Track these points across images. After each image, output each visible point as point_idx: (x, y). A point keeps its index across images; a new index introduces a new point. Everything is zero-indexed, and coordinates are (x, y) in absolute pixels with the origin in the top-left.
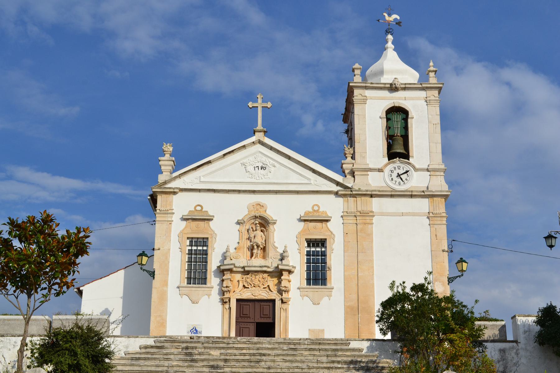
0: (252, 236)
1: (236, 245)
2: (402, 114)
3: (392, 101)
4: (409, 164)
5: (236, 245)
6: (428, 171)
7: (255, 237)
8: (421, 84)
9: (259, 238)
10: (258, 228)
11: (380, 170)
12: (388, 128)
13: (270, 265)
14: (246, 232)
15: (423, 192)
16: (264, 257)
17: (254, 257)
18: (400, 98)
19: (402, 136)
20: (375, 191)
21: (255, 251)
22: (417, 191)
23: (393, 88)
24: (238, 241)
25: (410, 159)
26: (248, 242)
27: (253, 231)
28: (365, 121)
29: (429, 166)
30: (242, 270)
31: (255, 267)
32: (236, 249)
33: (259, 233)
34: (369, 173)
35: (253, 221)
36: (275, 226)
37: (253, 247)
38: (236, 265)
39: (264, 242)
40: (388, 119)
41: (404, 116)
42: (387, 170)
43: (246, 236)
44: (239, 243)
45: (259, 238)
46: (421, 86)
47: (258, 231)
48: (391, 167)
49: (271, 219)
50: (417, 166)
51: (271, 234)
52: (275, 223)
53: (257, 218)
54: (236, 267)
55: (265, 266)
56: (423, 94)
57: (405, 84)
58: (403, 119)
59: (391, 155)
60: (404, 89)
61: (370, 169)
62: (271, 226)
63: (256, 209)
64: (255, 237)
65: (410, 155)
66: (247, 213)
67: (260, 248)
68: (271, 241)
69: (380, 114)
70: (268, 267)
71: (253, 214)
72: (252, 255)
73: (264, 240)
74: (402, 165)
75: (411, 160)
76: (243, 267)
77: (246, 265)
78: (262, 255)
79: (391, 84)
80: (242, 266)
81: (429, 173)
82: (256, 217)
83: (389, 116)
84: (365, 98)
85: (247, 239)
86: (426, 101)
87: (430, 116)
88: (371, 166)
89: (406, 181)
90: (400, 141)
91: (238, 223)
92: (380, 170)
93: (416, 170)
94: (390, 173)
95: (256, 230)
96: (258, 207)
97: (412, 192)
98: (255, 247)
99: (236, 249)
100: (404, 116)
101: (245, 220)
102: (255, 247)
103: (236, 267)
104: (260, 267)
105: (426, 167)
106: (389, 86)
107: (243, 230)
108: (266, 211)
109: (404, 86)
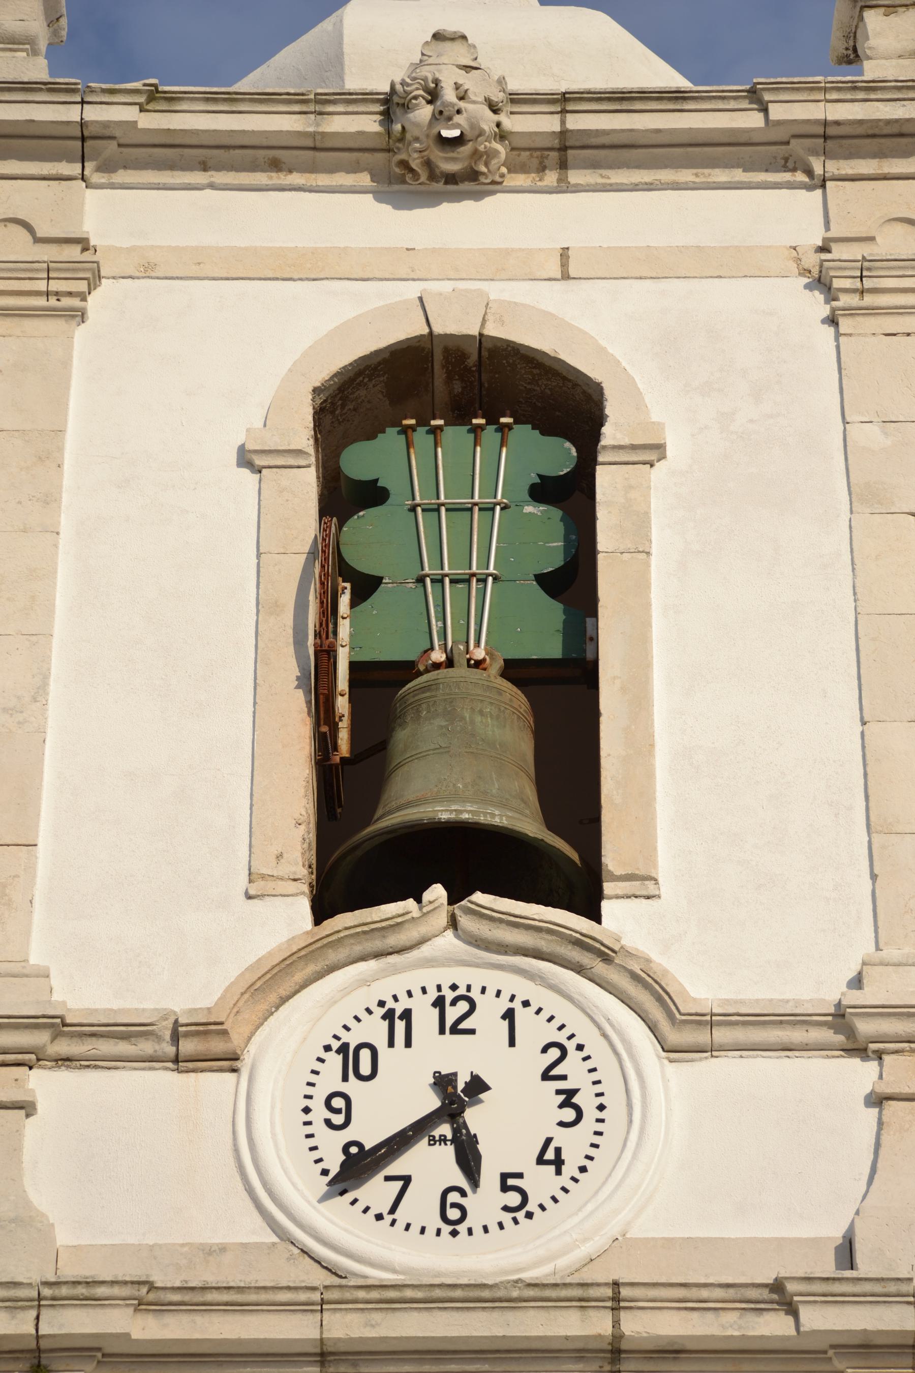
2: (524, 434)
3: (412, 290)
4: (596, 959)
6: (858, 1049)
8: (755, 98)
11: (200, 1046)
12: (342, 578)
15: (780, 1296)
18: (501, 264)
19: (517, 671)
20: (86, 1292)
22: (689, 1297)
23: (422, 150)
25: (606, 906)
28: (50, 500)
29: (857, 982)
34: (41, 1083)
40: (344, 498)
41: (559, 456)
42: (288, 1047)
46: (753, 120)
48: (342, 999)
50: (700, 986)
56: (787, 215)
57: (564, 101)
58: (544, 490)
59: (365, 857)
60: (560, 157)
61: (59, 1026)
65: (614, 855)
69: (242, 424)
74: (496, 982)
75: (619, 918)
79: (391, 105)
81: (862, 1075)
83: (361, 461)
84: (73, 252)
86: (821, 283)
87: (868, 436)
88: (80, 994)
89: (540, 1183)
90: (503, 724)
92: (200, 1046)
93: (688, 1032)
94: (331, 1077)
97: (616, 1299)
100: (559, 456)
105: (822, 988)
106: (369, 124)
109: (545, 123)
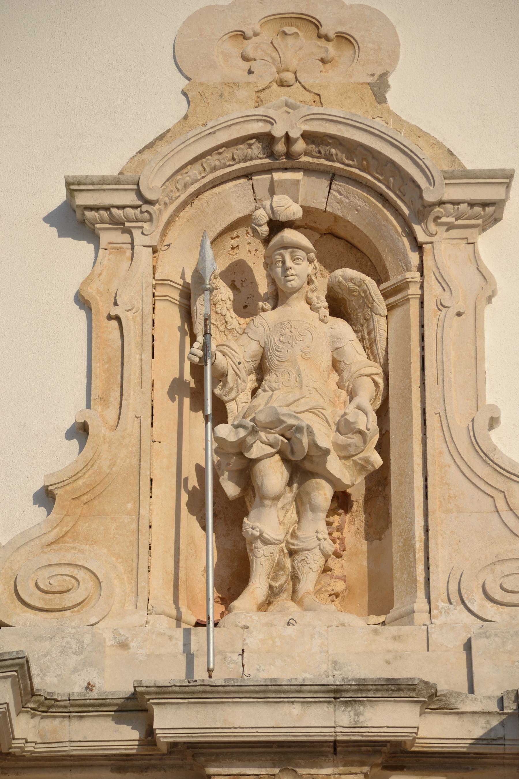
0: (234, 348)
1: (60, 457)
5: (60, 457)
7: (261, 370)
9: (311, 368)
10: (301, 269)
13: (447, 677)
14: (170, 316)
16: (380, 599)
17: (258, 587)
21: (268, 523)
24: (70, 415)
26: (195, 423)
27: (246, 308)
30: (125, 736)
31: (271, 692)
32: (46, 497)
33: (305, 329)
35: (236, 200)
36: (488, 244)
37: (247, 473)
38: (45, 681)
39: (369, 423)
43: (170, 362)
44: (81, 431)
45: (311, 368)
47: (296, 308)
49: (438, 166)
51: (446, 337)
52: (489, 212)
53: (290, 161)
54: (46, 706)
55: (393, 689)
62: (445, 250)
63: (266, 74)
64: (261, 370)
66: (170, 110)
67: (323, 494)
68: (450, 402)
70: (431, 699)
71: (239, 117)
72: (234, 578)
73: (367, 395)
76: (135, 707)
77: (172, 673)
78: (355, 566)
80: (117, 683)
82: (274, 152)
85: (177, 388)
91: (75, 220)
95: (278, 297)
96: (299, 49)
98: (273, 475)
99: (46, 497)
101: (153, 185)
102: (273, 475)
103: (46, 706)
104: (336, 694)
107: (133, 297)
108: (379, 88)
